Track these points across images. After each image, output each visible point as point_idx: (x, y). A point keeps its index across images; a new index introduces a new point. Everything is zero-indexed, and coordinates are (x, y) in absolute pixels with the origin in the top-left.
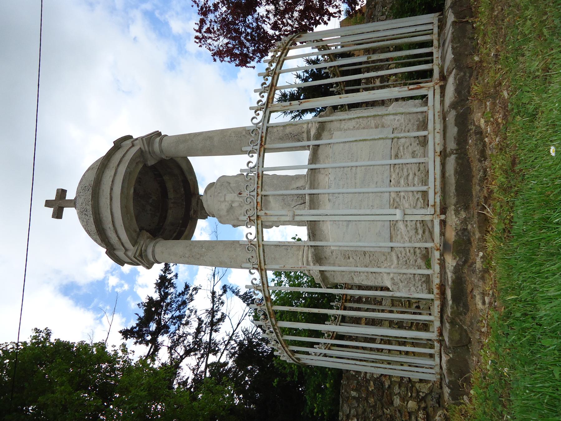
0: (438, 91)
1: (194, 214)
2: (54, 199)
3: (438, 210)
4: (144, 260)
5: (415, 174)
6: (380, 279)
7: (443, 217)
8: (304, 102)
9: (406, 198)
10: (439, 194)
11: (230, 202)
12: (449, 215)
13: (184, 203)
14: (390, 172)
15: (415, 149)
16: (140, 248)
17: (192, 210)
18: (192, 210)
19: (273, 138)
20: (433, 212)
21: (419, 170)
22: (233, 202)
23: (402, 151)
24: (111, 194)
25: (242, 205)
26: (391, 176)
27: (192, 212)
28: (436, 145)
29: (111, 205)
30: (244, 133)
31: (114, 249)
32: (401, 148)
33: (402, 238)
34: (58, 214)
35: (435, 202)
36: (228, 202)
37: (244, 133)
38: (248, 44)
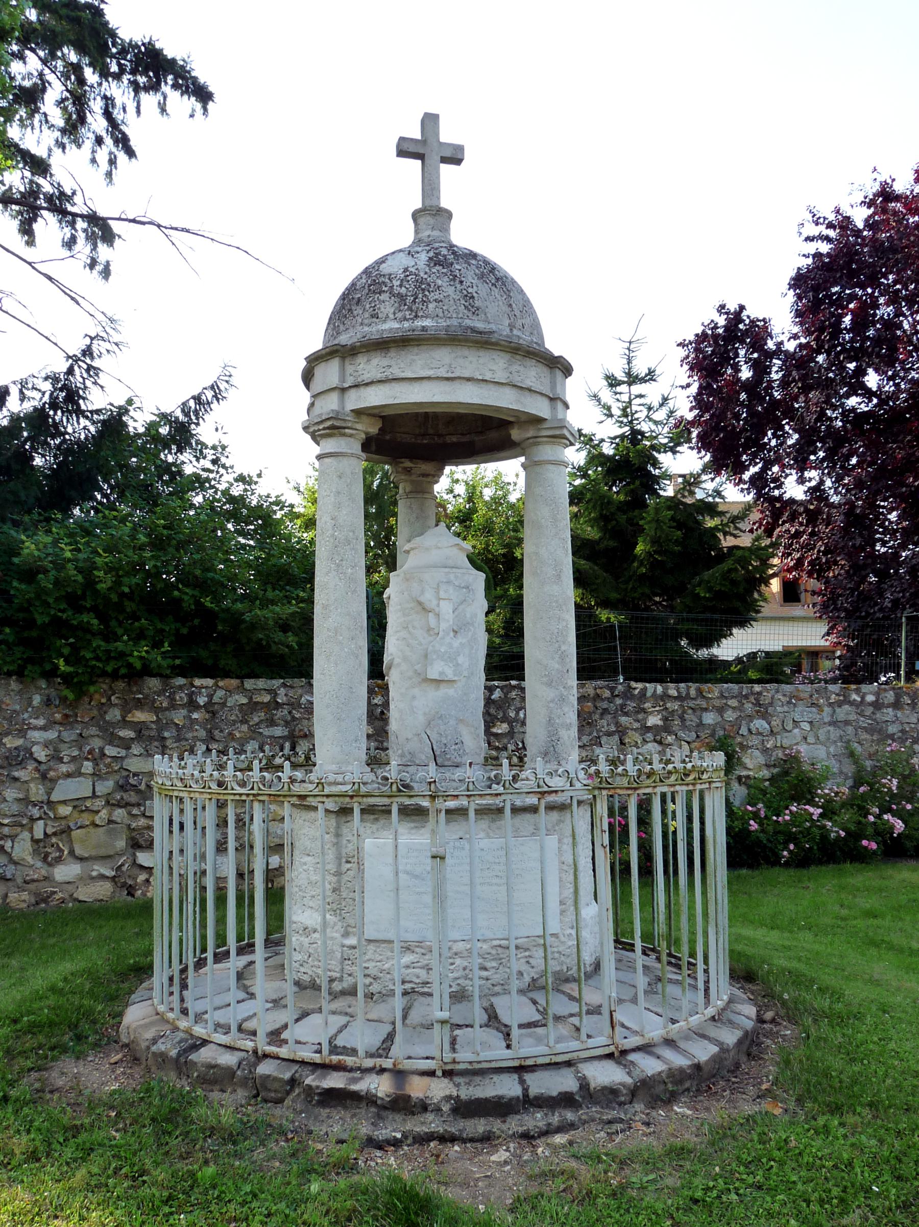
0: (607, 1051)
1: (405, 468)
2: (443, 139)
3: (449, 1067)
4: (324, 429)
5: (487, 979)
6: (311, 904)
7: (439, 1073)
8: (605, 853)
9: (452, 967)
10: (470, 1067)
11: (437, 610)
12: (443, 1085)
13: (425, 442)
14: (492, 940)
15: (525, 975)
16: (350, 425)
17: (412, 465)
18: (412, 465)
19: (551, 705)
20: (445, 1060)
21: (493, 985)
22: (438, 615)
23: (523, 955)
24: (460, 378)
25: (431, 633)
26: (485, 941)
27: (408, 464)
28: (534, 1059)
29: (438, 378)
30: (563, 648)
31: (343, 358)
32: (527, 954)
33: (388, 958)
34: (405, 150)
35: (459, 1063)
36: (438, 605)
37: (563, 648)
38: (618, 1179)
